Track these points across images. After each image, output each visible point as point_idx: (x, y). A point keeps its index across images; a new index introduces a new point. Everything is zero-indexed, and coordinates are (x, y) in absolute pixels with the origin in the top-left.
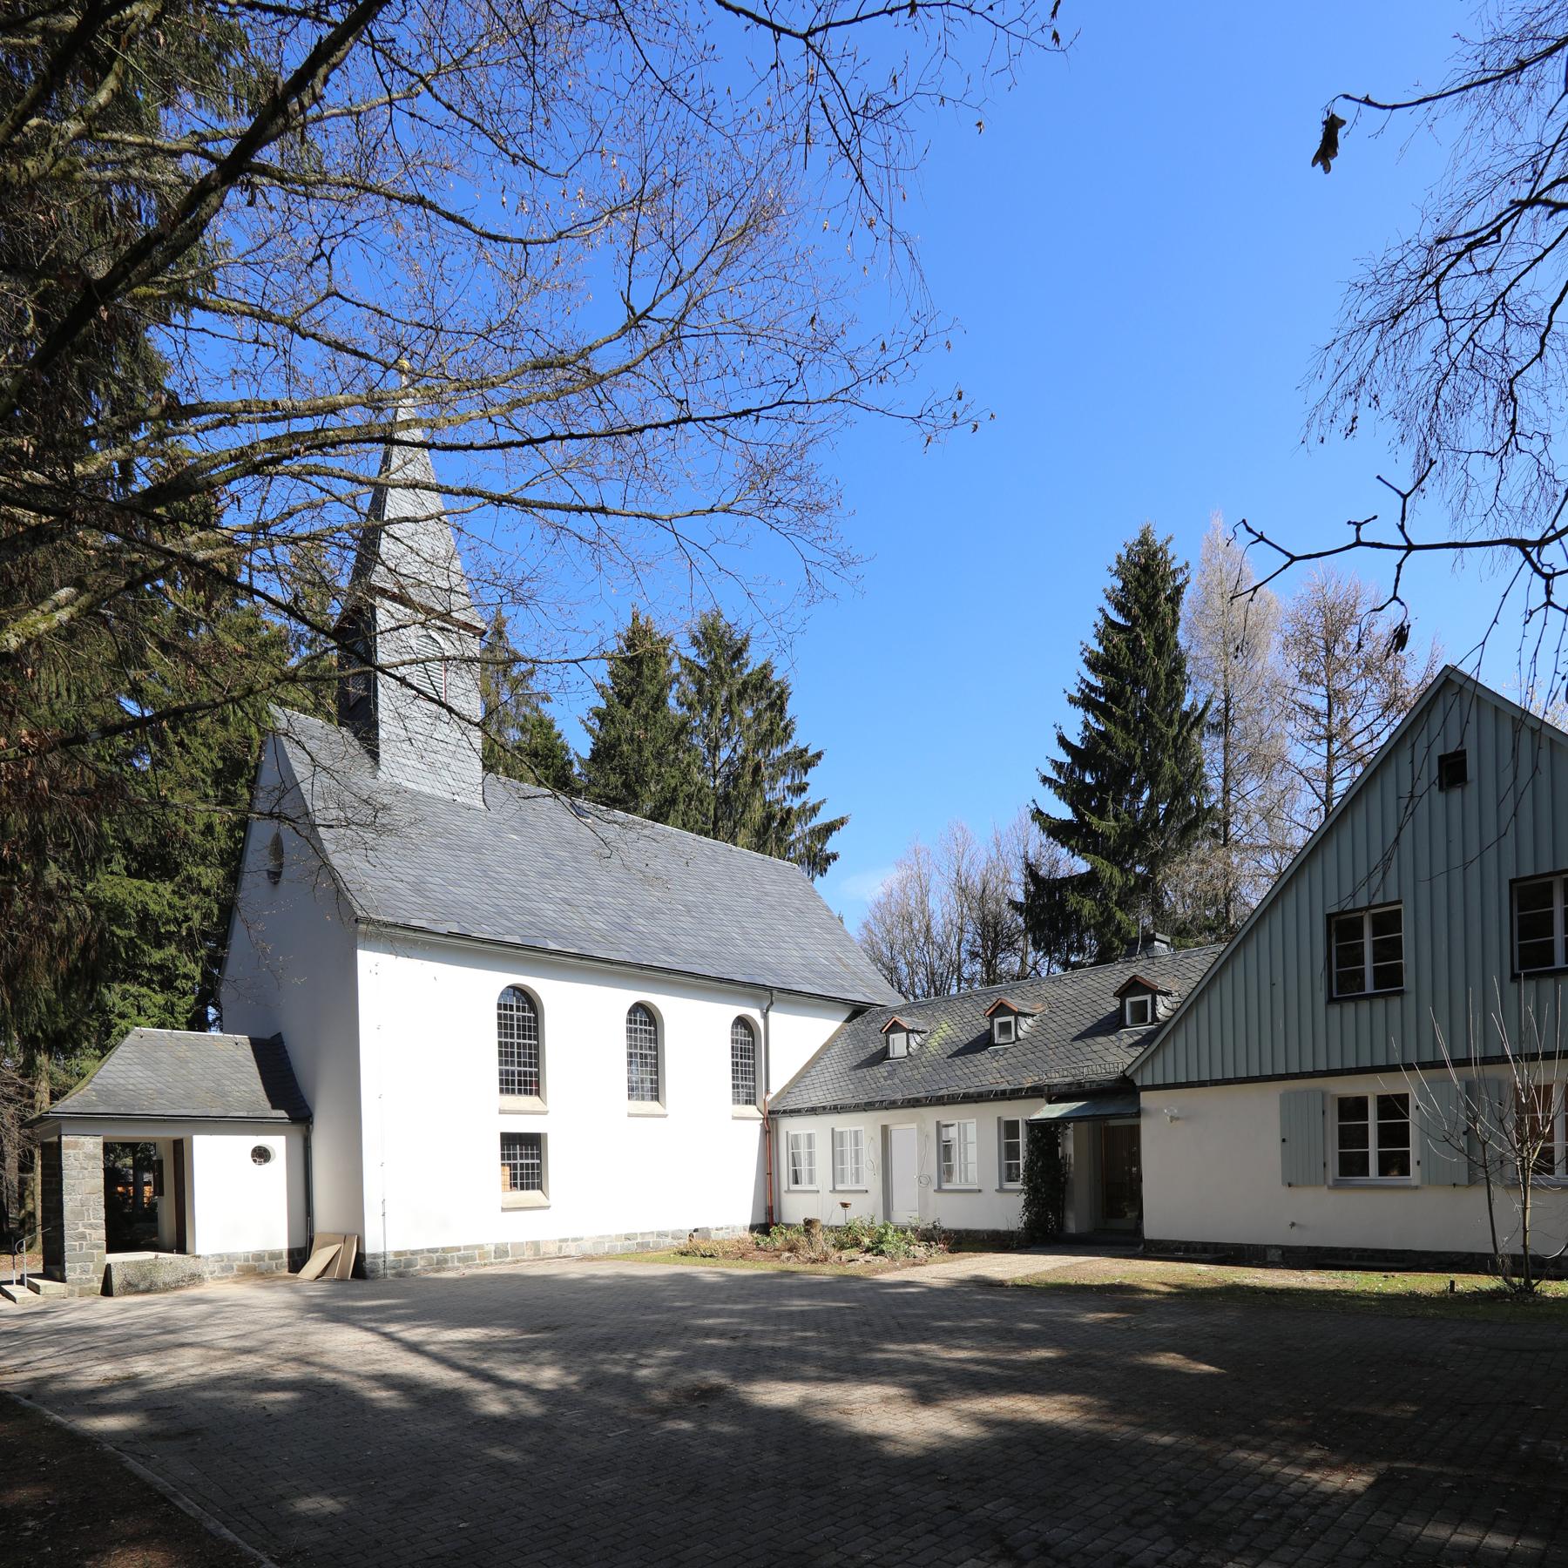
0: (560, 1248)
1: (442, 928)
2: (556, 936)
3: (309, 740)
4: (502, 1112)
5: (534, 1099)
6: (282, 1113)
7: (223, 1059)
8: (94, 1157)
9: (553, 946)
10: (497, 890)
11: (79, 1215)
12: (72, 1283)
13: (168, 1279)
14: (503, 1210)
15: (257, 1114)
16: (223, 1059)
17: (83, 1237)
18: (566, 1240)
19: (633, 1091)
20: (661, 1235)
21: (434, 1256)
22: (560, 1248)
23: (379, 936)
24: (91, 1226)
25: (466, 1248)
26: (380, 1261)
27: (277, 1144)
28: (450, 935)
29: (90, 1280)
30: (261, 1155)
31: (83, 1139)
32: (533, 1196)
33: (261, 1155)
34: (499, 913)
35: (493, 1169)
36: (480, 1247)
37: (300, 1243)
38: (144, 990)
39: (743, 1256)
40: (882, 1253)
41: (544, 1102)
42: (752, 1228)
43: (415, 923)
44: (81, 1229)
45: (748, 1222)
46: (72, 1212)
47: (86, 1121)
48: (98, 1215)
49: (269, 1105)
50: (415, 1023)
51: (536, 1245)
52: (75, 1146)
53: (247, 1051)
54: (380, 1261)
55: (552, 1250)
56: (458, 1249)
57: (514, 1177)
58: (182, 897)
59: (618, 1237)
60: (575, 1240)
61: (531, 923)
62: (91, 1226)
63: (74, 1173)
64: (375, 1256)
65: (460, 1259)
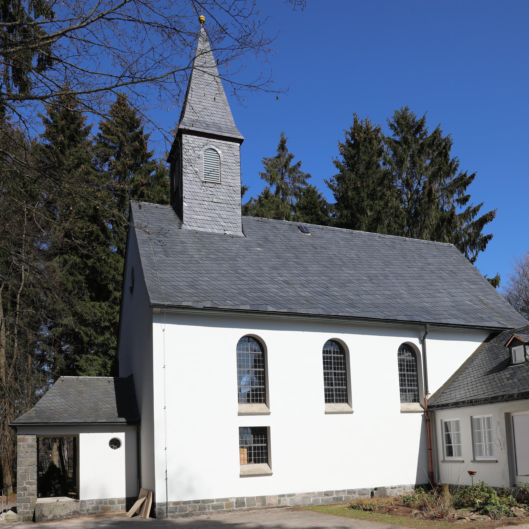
0: (279, 501)
1: (200, 305)
2: (274, 303)
3: (147, 215)
4: (240, 414)
5: (263, 405)
6: (123, 420)
7: (97, 389)
8: (32, 446)
9: (270, 309)
10: (242, 280)
11: (24, 477)
12: (20, 514)
13: (62, 514)
14: (241, 476)
15: (112, 420)
16: (97, 389)
17: (25, 489)
18: (283, 496)
19: (329, 398)
20: (350, 492)
21: (197, 505)
22: (279, 501)
23: (162, 313)
24: (30, 484)
25: (217, 500)
26: (164, 508)
27: (121, 436)
28: (205, 309)
29: (28, 513)
30: (115, 443)
31: (27, 437)
32: (262, 467)
33: (115, 443)
34: (240, 294)
35: (233, 449)
36: (227, 500)
37: (133, 495)
38: (95, 357)
39: (390, 511)
40: (486, 512)
41: (268, 406)
42: (417, 487)
43: (184, 304)
44: (25, 485)
45: (414, 482)
46: (21, 476)
47: (29, 427)
48: (33, 478)
49: (117, 414)
50: (189, 364)
51: (263, 499)
52: (23, 440)
53: (112, 386)
54: (164, 508)
55: (274, 502)
56: (212, 501)
57: (249, 455)
58: (112, 308)
59: (320, 494)
60: (290, 495)
61: (260, 297)
62: (30, 484)
63: (22, 455)
64: (161, 504)
65: (214, 507)
